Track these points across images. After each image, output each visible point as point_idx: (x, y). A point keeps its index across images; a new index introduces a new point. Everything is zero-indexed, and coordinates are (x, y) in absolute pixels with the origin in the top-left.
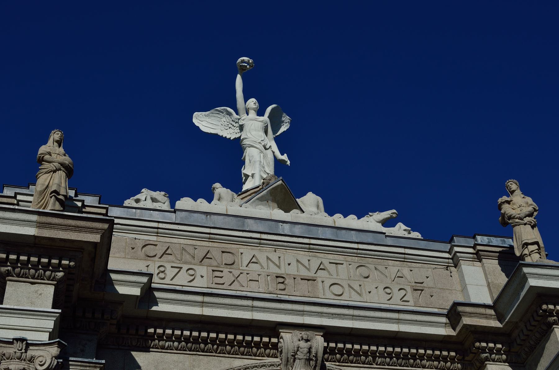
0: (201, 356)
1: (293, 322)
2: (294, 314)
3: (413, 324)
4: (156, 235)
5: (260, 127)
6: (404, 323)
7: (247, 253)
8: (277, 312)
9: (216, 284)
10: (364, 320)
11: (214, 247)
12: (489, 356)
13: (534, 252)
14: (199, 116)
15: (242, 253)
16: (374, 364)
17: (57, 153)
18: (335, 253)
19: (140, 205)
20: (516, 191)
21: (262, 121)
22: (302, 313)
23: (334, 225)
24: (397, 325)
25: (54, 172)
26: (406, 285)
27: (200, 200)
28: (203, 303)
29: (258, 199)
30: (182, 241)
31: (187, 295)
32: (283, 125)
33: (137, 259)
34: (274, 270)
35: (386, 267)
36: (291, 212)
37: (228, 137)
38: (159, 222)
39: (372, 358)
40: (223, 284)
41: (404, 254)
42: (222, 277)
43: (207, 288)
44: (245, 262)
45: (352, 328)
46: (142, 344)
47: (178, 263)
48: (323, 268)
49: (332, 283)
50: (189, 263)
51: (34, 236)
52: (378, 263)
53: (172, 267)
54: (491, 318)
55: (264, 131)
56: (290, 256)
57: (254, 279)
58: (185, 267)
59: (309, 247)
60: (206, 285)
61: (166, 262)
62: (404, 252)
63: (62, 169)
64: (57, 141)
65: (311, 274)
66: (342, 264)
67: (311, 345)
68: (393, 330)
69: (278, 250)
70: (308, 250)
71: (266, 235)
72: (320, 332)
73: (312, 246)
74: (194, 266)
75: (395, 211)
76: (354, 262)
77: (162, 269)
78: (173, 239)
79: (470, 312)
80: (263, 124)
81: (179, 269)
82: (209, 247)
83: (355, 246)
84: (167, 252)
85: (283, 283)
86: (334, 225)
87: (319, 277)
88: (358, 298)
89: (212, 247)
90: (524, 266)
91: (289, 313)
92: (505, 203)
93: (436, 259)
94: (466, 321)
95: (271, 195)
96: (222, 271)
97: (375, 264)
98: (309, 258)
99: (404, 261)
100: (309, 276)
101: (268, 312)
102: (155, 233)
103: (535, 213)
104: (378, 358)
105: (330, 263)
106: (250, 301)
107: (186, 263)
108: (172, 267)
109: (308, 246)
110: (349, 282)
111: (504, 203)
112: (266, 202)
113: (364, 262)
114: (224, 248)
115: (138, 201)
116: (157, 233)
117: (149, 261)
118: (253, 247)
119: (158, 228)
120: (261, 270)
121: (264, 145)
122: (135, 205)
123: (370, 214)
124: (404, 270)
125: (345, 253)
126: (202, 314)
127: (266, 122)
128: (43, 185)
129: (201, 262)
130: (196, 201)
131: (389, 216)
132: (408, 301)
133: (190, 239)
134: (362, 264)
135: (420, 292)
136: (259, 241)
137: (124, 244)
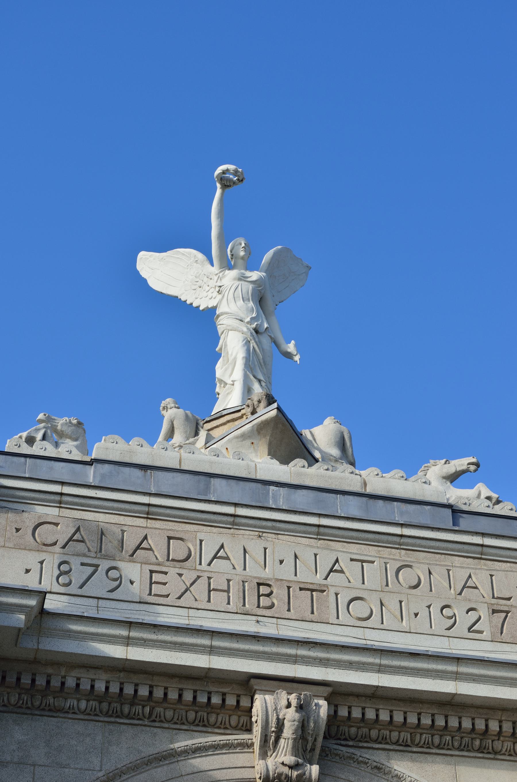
0: (122, 726)
1: (278, 674)
9: (156, 595)
11: (156, 528)
14: (148, 259)
15: (201, 541)
22: (295, 660)
23: (362, 491)
24: (454, 682)
27: (135, 441)
29: (237, 437)
30: (101, 517)
33: (25, 549)
35: (449, 568)
36: (292, 463)
37: (194, 305)
38: (63, 483)
40: (167, 596)
42: (165, 584)
45: (377, 687)
46: (27, 703)
47: (92, 557)
50: (111, 557)
52: (436, 561)
53: (82, 564)
57: (219, 588)
58: (104, 565)
61: (73, 555)
66: (373, 562)
68: (446, 691)
76: (394, 559)
78: (86, 513)
80: (256, 286)
82: (146, 527)
83: (397, 530)
85: (269, 595)
86: (363, 491)
87: (330, 585)
89: (151, 528)
96: (166, 573)
97: (429, 564)
98: (316, 551)
99: (481, 559)
102: (56, 503)
105: (352, 560)
107: (107, 557)
108: (82, 564)
110: (382, 595)
113: (411, 557)
117: (44, 554)
119: (61, 494)
126: (125, 658)
129: (132, 555)
130: (128, 441)
132: (481, 632)
134: (406, 563)
135: (504, 615)
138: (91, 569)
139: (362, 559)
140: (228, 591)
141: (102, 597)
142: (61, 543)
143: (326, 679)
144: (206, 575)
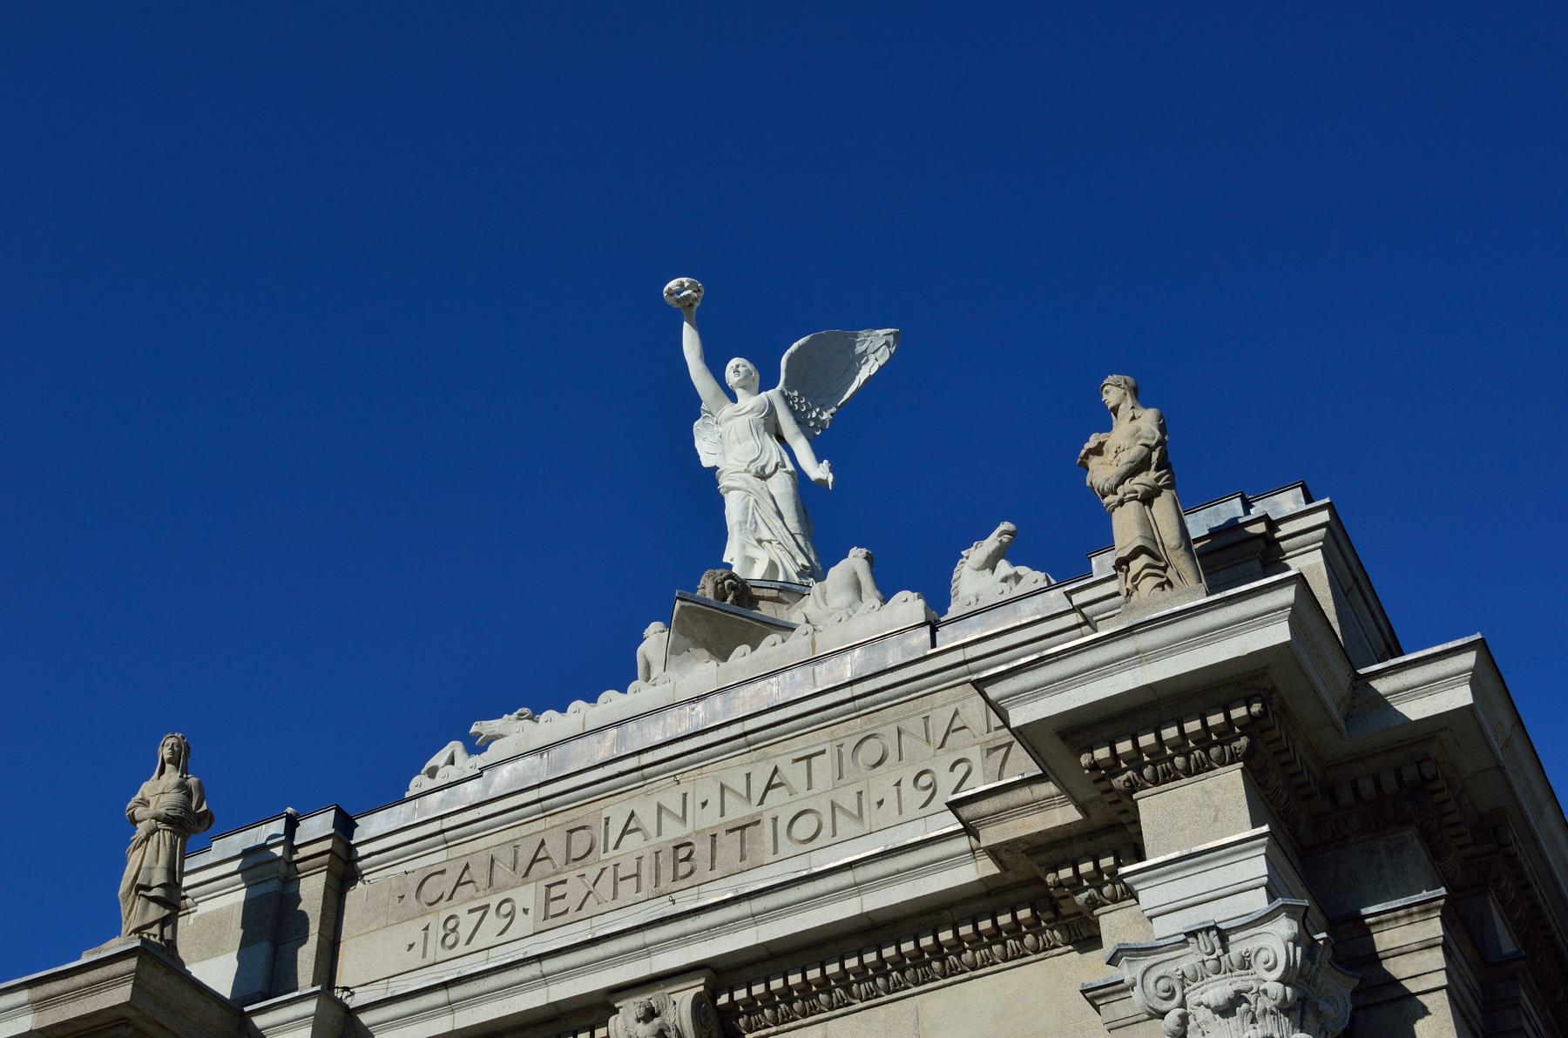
2: (631, 960)
3: (895, 881)
4: (445, 846)
5: (747, 428)
6: (873, 888)
7: (616, 810)
8: (596, 969)
9: (553, 916)
10: (782, 915)
12: (1096, 894)
13: (1140, 577)
16: (855, 1001)
17: (160, 791)
18: (808, 729)
19: (439, 780)
20: (1121, 407)
21: (752, 409)
22: (646, 950)
25: (147, 839)
26: (972, 746)
28: (450, 1003)
31: (417, 1000)
32: (867, 361)
33: (408, 920)
34: (674, 831)
38: (441, 817)
39: (842, 992)
40: (566, 911)
41: (966, 662)
42: (563, 897)
43: (535, 934)
44: (612, 841)
48: (777, 782)
49: (794, 815)
51: (31, 1031)
53: (471, 911)
54: (1055, 804)
55: (762, 429)
56: (702, 784)
58: (494, 901)
59: (746, 741)
60: (532, 928)
62: (961, 659)
63: (159, 827)
64: (170, 761)
65: (750, 811)
66: (823, 752)
67: (659, 1025)
69: (685, 775)
70: (747, 749)
71: (650, 753)
72: (698, 978)
73: (750, 737)
74: (510, 891)
75: (1006, 526)
77: (451, 924)
79: (994, 811)
81: (483, 911)
83: (845, 694)
84: (462, 882)
88: (858, 829)
89: (553, 827)
90: (985, 682)
91: (619, 962)
92: (1091, 456)
93: (1048, 640)
94: (992, 835)
95: (685, 636)
96: (564, 882)
97: (895, 721)
100: (741, 819)
101: (579, 974)
103: (1155, 455)
104: (855, 985)
106: (535, 965)
109: (742, 740)
111: (1086, 456)
112: (686, 653)
114: (568, 822)
115: (432, 773)
116: (446, 842)
117: (429, 916)
118: (632, 792)
120: (646, 844)
121: (757, 472)
122: (428, 784)
123: (963, 553)
124: (970, 705)
125: (829, 719)
127: (762, 408)
128: (130, 877)
129: (526, 875)
131: (997, 544)
133: (508, 828)
134: (870, 733)
136: (640, 772)
137: (386, 895)
138: (479, 914)
139: (807, 754)
140: (637, 875)
141: (492, 945)
142: (446, 896)
143: (689, 962)
144: (610, 864)
